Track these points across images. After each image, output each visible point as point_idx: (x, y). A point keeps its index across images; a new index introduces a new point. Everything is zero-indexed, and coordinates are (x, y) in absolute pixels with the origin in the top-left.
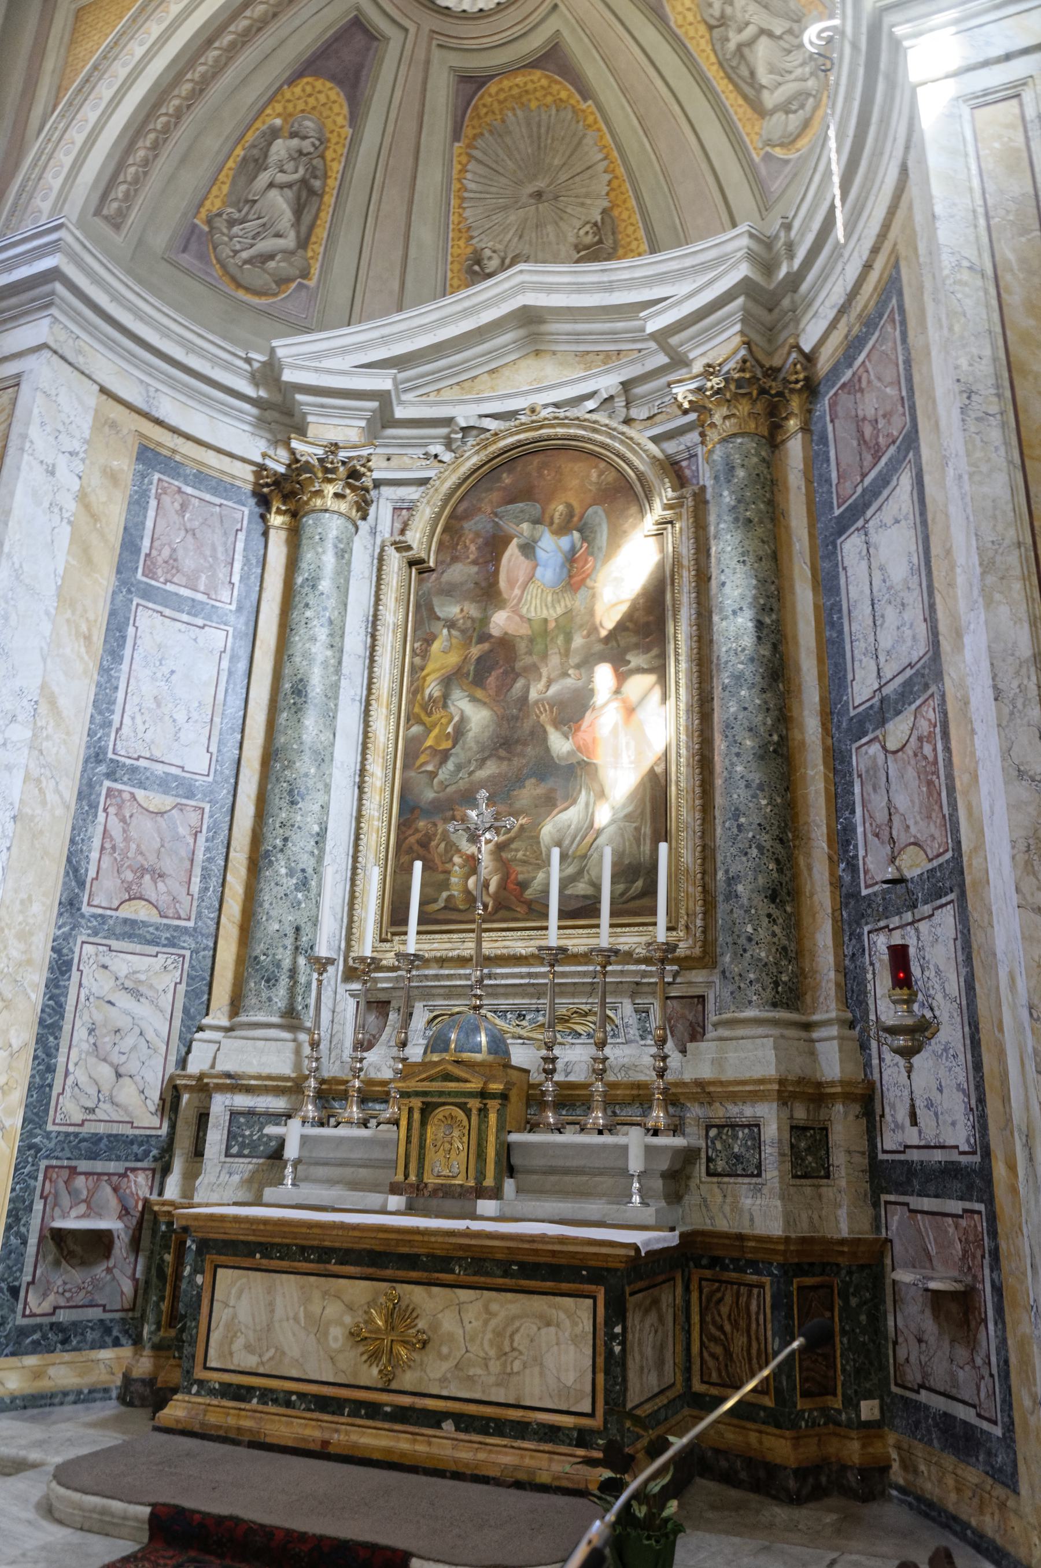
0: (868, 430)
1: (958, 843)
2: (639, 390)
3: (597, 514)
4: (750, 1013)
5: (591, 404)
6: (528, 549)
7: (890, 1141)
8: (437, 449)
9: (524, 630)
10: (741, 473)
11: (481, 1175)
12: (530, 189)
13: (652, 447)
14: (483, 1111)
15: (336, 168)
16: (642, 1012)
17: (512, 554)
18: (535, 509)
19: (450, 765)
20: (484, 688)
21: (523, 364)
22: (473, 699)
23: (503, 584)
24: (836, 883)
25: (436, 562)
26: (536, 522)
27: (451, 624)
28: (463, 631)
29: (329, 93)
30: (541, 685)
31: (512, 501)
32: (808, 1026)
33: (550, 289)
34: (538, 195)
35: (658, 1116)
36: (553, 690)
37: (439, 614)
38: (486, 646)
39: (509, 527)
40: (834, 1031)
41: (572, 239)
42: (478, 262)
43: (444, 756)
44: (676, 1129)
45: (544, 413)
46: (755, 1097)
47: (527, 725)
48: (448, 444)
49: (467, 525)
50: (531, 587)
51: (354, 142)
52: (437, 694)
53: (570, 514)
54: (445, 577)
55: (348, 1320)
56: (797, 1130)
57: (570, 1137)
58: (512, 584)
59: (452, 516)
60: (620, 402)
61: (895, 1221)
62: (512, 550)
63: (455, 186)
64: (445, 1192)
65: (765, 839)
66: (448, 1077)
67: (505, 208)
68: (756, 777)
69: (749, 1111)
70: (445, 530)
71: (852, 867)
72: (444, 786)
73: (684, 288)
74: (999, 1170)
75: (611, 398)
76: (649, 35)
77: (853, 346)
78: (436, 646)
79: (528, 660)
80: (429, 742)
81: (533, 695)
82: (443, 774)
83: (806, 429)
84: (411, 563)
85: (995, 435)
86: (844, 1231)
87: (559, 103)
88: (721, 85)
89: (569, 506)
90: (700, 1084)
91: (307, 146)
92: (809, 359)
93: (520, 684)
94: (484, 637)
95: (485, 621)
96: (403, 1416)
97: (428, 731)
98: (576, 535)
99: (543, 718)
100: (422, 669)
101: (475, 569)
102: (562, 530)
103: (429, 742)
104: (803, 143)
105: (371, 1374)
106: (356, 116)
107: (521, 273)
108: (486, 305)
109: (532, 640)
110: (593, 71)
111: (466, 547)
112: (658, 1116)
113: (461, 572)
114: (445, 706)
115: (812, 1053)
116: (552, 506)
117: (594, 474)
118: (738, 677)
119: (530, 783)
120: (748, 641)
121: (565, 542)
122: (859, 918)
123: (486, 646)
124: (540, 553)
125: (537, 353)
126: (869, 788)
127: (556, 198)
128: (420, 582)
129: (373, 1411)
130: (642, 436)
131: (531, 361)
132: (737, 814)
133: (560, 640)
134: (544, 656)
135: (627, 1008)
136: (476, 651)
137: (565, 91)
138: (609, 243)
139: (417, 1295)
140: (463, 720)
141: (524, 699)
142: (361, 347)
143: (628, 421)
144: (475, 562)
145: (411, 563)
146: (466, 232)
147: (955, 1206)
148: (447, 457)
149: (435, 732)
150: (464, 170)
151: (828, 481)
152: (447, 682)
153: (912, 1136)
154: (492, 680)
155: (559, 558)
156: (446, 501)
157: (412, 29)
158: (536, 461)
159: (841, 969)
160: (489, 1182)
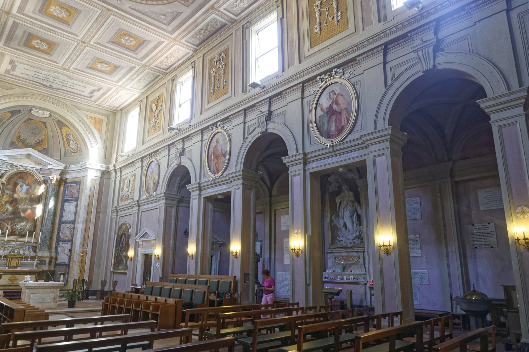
0: (72, 193)
1: (73, 239)
2: (42, 170)
3: (32, 184)
4: (46, 250)
5: (35, 169)
6: (21, 186)
7: (58, 262)
8: (9, 166)
9: (19, 198)
10: (56, 190)
11: (18, 265)
12: (32, 132)
13: (42, 178)
14: (19, 259)
15: (4, 121)
16: (29, 248)
17: (18, 186)
18: (23, 181)
19: (5, 214)
20: (12, 204)
21: (26, 159)
22: (10, 206)
23: (17, 190)
24: (57, 238)
25: (6, 184)
26: (23, 183)
27: (7, 194)
28: (9, 196)
29: (10, 115)
30: (21, 206)
31: (20, 178)
32: (51, 251)
33: (34, 153)
34: (33, 133)
35: (36, 259)
36: (22, 207)
37: (5, 192)
38: (13, 199)
39: (19, 182)
40: (54, 252)
41: (36, 140)
42: (20, 137)
43: (4, 213)
44: (38, 261)
45: (28, 168)
46: (47, 258)
47: (18, 211)
48: (11, 166)
49: (12, 180)
50: (21, 192)
51: (8, 119)
52: (4, 204)
53: (29, 183)
54: (7, 187)
55: (8, 278)
56: (49, 261)
57: (26, 261)
58: (18, 191)
59: (9, 178)
60: (39, 170)
61: (57, 269)
62: (19, 186)
63: (21, 127)
64: (13, 267)
65: (51, 232)
66: (15, 256)
67: (27, 132)
68: (51, 226)
69: (45, 259)
70: (8, 179)
71: (59, 236)
72: (4, 217)
73: (55, 165)
74: (71, 264)
75: (38, 169)
76: (58, 130)
77: (72, 183)
78: (4, 197)
79: (19, 202)
80: (2, 210)
81: (19, 207)
82: (4, 215)
83: (64, 187)
84: (2, 183)
85: (86, 211)
86: (52, 269)
87: (41, 126)
88: (65, 139)
89: (29, 182)
90: (40, 257)
91: (2, 118)
92: (66, 179)
93: (17, 205)
94: (13, 197)
95: (13, 195)
96: (14, 286)
97: (2, 209)
98: (29, 187)
99: (20, 211)
100: (2, 199)
101: (12, 187)
102: (27, 185)
103: (2, 210)
104: (73, 154)
105: (11, 283)
106: (11, 117)
107: (30, 149)
108: (24, 151)
109: (20, 200)
110: (49, 127)
111: (11, 183)
112: (36, 259)
113: (10, 187)
114: (5, 206)
115: (51, 254)
116: (26, 181)
117: (33, 179)
118: (51, 215)
119: (17, 219)
120: (53, 211)
121: (27, 187)
122: (59, 241)
123: (13, 199)
124: (23, 188)
125: (28, 158)
126: (63, 230)
127: (35, 134)
128: (3, 186)
129: (11, 286)
130: (41, 176)
131: (27, 159)
132: (48, 229)
133: (24, 201)
134: (22, 202)
135: (27, 247)
136: (11, 199)
137: (43, 125)
138: (41, 144)
139: (16, 276)
140: (8, 208)
141: (18, 207)
142: (4, 153)
143: (39, 173)
144: (12, 186)
145: (2, 183)
146: (20, 133)
147: (65, 267)
148: (10, 168)
149: (3, 209)
150: (23, 126)
151: (65, 194)
152: (6, 202)
153: (61, 261)
154: (13, 204)
155: (26, 189)
156: (9, 175)
157: (26, 113)
158: (24, 174)
159: (56, 246)
160: (19, 266)
